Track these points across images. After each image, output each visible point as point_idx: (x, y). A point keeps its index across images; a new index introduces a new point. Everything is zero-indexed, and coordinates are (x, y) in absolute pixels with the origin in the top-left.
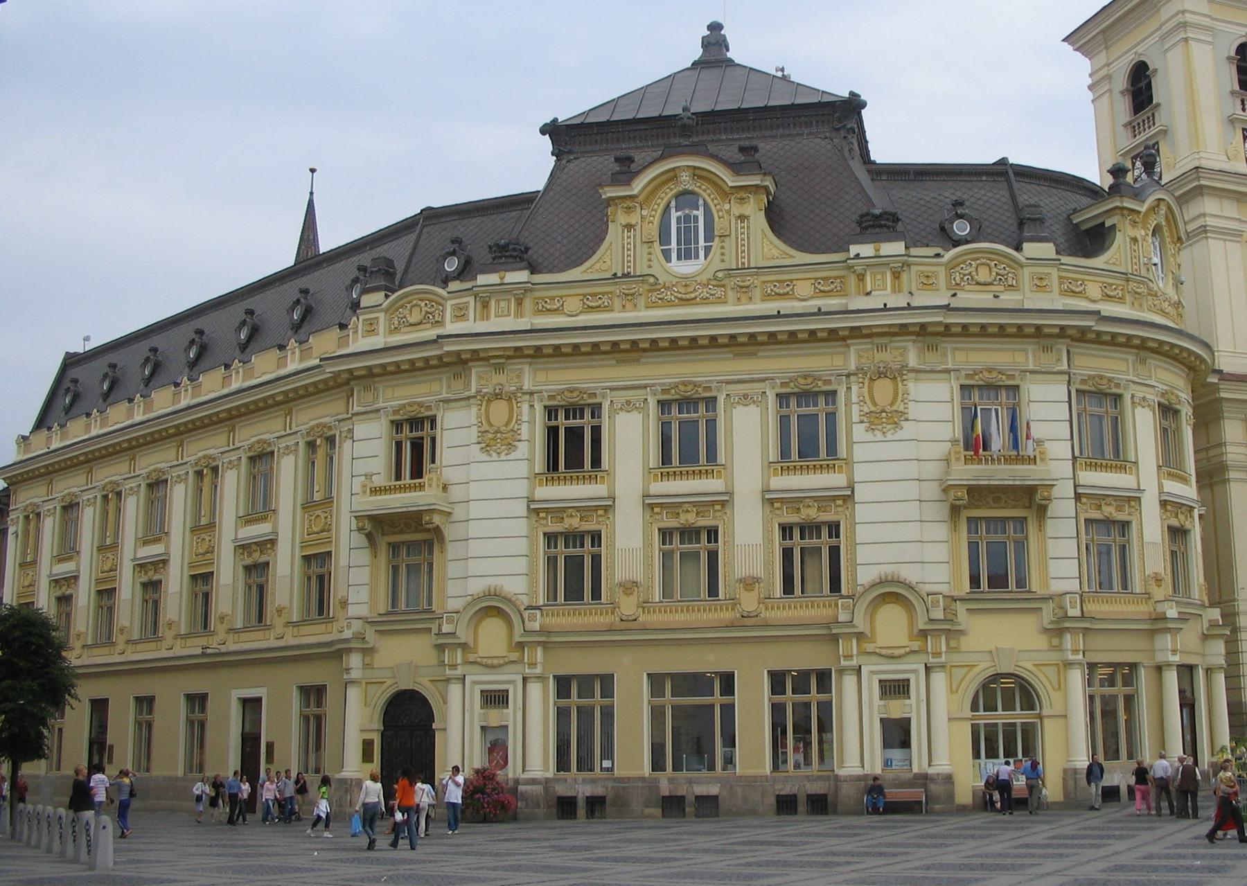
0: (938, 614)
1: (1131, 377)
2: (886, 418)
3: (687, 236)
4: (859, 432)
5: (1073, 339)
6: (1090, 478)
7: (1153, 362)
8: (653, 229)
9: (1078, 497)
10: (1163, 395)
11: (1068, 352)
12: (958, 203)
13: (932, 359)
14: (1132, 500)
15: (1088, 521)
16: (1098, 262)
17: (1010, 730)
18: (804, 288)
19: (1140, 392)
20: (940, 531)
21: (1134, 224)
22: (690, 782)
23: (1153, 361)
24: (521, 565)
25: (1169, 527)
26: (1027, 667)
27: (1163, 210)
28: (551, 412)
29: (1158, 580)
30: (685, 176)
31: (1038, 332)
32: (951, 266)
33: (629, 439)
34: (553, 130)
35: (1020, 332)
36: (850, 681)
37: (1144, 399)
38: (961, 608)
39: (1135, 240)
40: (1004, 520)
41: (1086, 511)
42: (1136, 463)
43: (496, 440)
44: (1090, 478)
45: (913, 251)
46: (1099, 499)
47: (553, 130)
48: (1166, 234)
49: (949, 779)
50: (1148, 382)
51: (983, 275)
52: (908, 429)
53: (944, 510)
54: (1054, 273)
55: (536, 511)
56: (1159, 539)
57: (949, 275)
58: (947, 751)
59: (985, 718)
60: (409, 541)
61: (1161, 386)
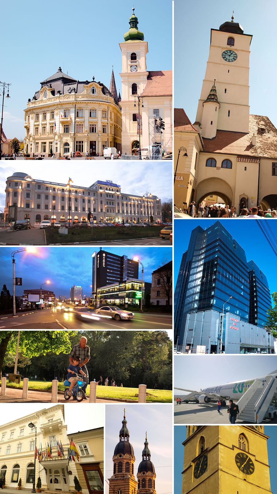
0: (59, 136)
2: (57, 114)
3: (46, 95)
4: (55, 116)
6: (77, 119)
8: (43, 95)
9: (75, 122)
11: (75, 105)
12: (70, 88)
13: (61, 107)
16: (81, 94)
17: (67, 148)
18: (53, 100)
19: (86, 108)
20: (61, 126)
22: (43, 153)
24: (33, 131)
25: (90, 125)
26: (68, 142)
27: (94, 85)
28: (36, 115)
29: (86, 131)
30: (45, 88)
31: (71, 103)
32: (64, 96)
33: (41, 116)
34: (41, 83)
35: (69, 103)
36: (53, 143)
39: (87, 90)
40: (68, 125)
43: (32, 118)
45: (61, 95)
47: (41, 83)
51: (67, 97)
52: (59, 115)
53: (61, 124)
54: (74, 96)
55: (35, 125)
57: (64, 97)
58: (61, 150)
59: (66, 147)
60: (28, 129)
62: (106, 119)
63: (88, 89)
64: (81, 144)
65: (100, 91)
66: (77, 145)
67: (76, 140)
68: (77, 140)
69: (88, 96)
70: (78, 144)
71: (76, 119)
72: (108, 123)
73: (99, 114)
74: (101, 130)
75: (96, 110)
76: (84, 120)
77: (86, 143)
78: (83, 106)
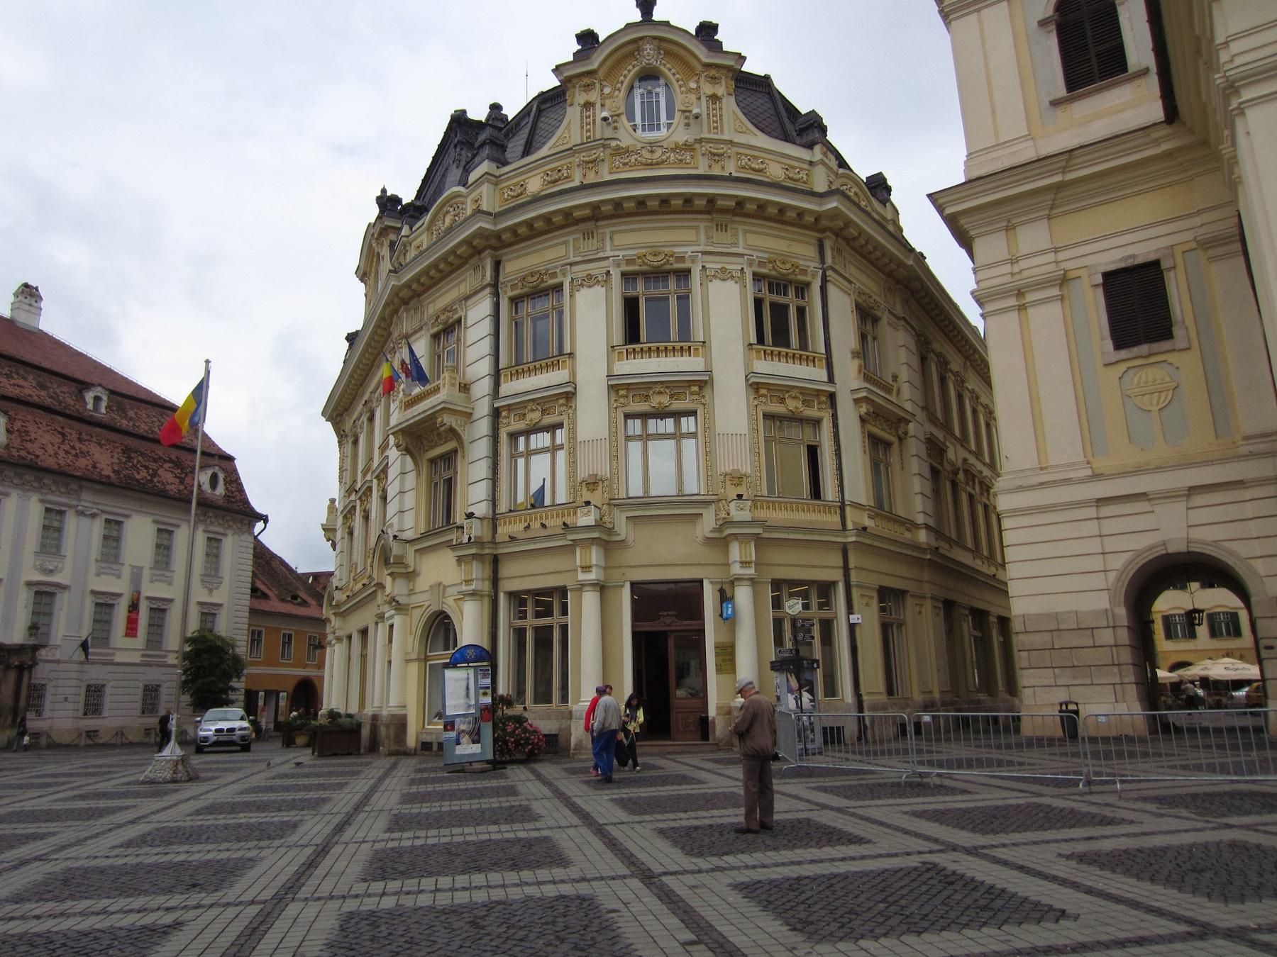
1: (572, 259)
5: (496, 249)
7: (608, 231)
9: (496, 414)
10: (630, 262)
11: (497, 265)
14: (702, 384)
15: (767, 416)
21: (588, 88)
23: (607, 229)
27: (648, 49)
37: (589, 277)
38: (411, 550)
39: (588, 105)
41: (508, 424)
42: (571, 355)
44: (509, 387)
46: (519, 408)
48: (669, 74)
49: (400, 724)
50: (601, 255)
56: (605, 433)
61: (621, 253)
62: (810, 360)
63: (593, 96)
64: (555, 620)
65: (714, 98)
66: (520, 633)
67: (507, 585)
68: (519, 577)
69: (600, 153)
70: (531, 622)
71: (508, 387)
72: (832, 396)
73: (724, 310)
74: (746, 468)
75: (684, 274)
76: (572, 382)
77: (590, 600)
78: (560, 251)
